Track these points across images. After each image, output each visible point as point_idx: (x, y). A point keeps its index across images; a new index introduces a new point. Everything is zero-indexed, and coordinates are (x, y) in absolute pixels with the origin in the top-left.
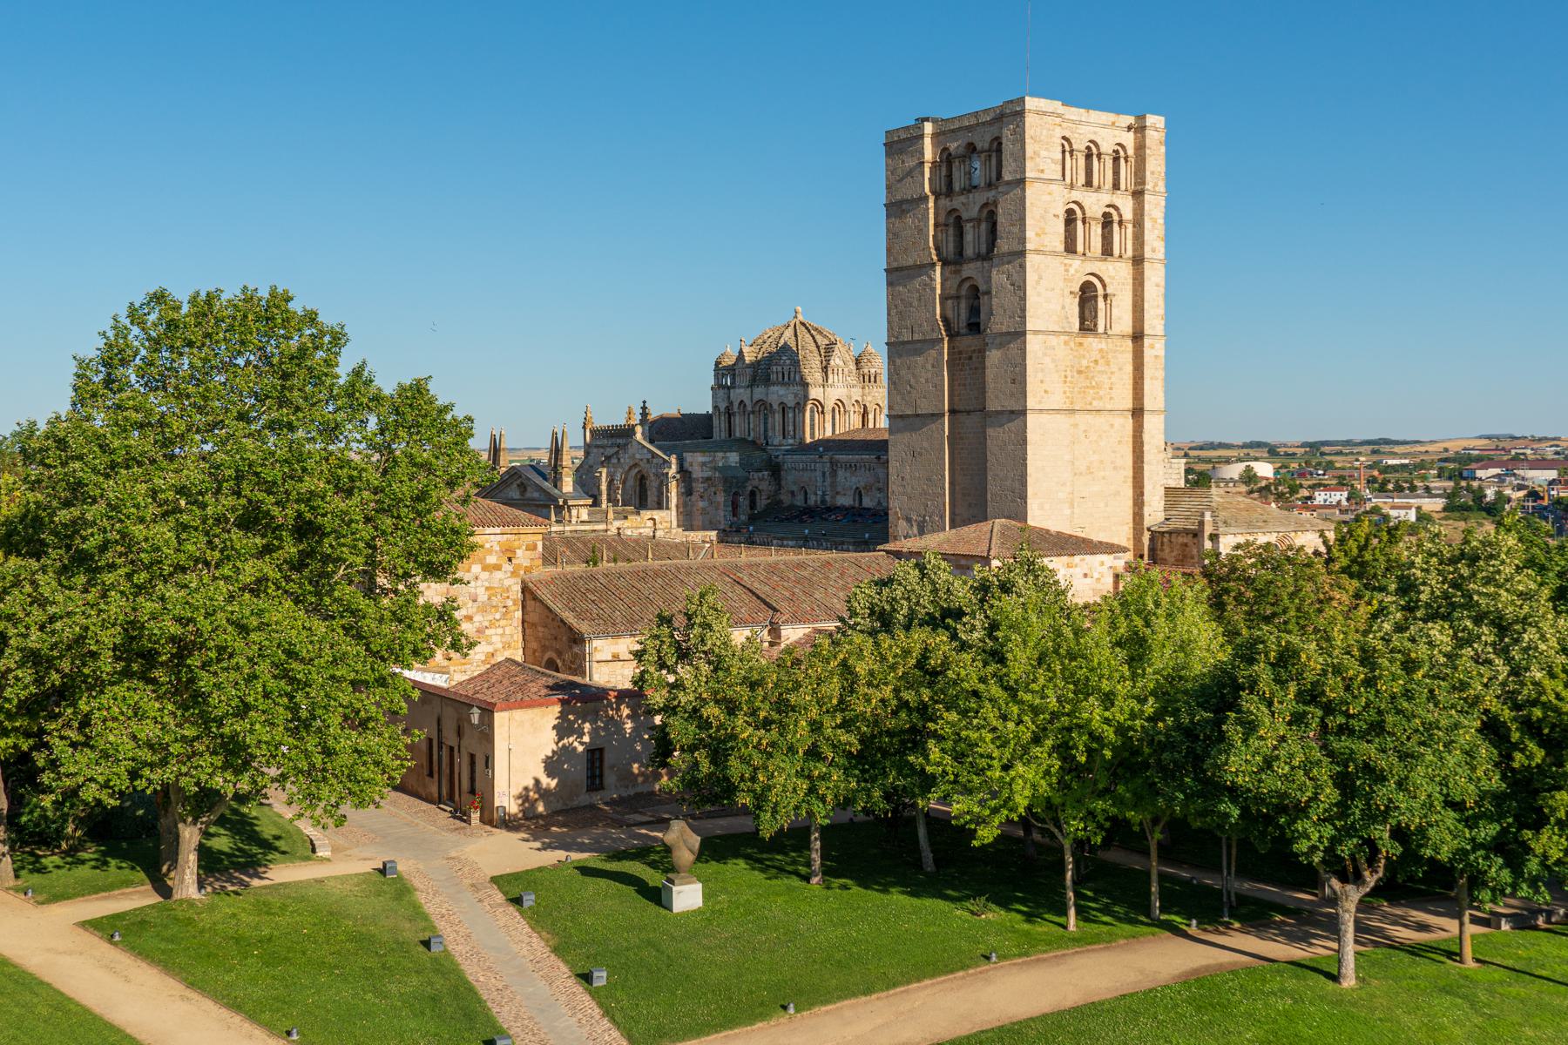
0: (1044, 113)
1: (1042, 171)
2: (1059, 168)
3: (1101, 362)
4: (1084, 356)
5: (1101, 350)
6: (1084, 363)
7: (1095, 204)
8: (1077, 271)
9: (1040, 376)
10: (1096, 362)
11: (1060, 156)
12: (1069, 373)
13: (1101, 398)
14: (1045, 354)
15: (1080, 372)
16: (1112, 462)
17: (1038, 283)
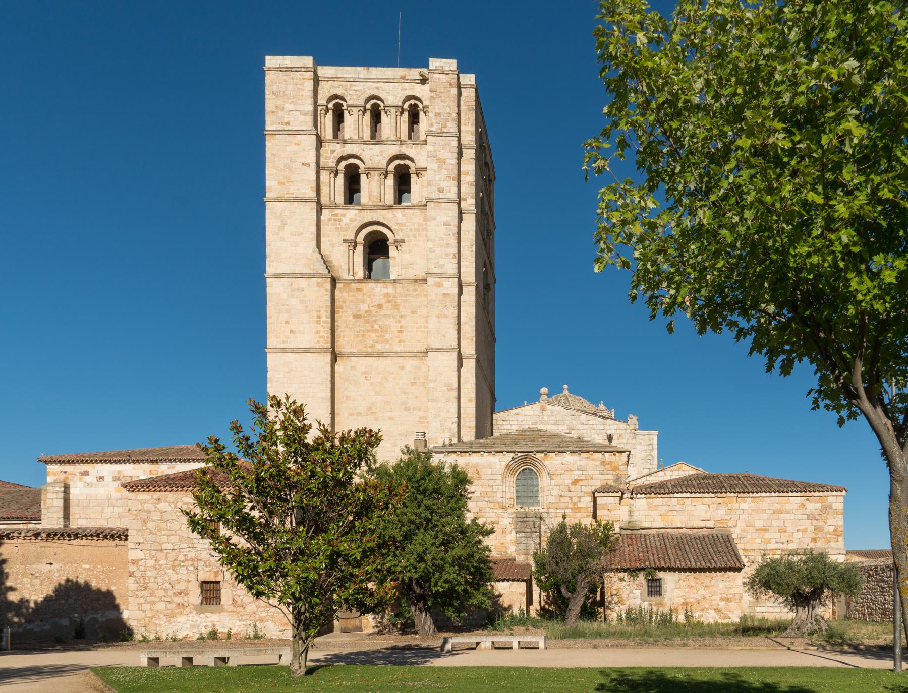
6: (364, 307)
8: (352, 220)
9: (284, 317)
13: (387, 341)
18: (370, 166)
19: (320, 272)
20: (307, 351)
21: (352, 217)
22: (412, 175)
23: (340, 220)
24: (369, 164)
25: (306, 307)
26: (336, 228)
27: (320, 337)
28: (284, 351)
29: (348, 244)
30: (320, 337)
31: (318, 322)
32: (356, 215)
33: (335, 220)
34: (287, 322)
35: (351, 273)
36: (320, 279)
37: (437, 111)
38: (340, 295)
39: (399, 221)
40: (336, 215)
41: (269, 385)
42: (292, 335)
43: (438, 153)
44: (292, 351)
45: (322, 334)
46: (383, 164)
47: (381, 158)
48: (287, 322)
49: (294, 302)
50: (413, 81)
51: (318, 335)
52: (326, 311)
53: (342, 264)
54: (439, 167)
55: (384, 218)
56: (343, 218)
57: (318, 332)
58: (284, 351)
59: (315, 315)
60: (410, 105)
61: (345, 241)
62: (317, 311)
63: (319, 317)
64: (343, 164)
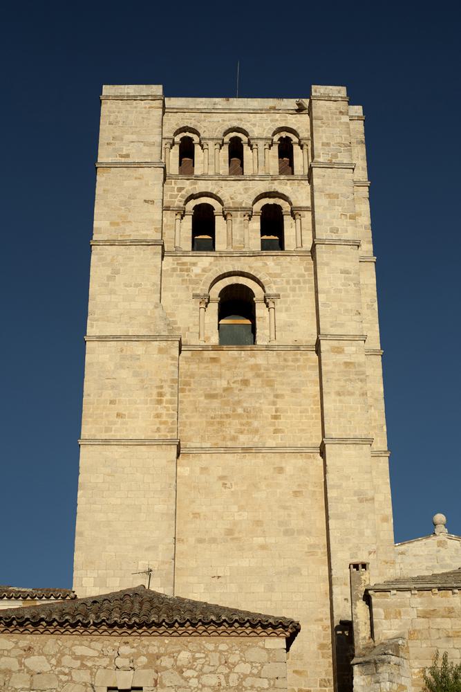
0: (134, 98)
1: (127, 156)
2: (156, 150)
4: (220, 376)
5: (255, 367)
7: (238, 193)
8: (204, 270)
9: (109, 394)
10: (245, 382)
11: (158, 139)
12: (166, 390)
14: (122, 367)
15: (211, 396)
16: (281, 523)
17: (110, 278)
18: (231, 205)
19: (163, 333)
20: (141, 443)
21: (205, 265)
23: (188, 270)
24: (228, 203)
25: (142, 381)
26: (183, 280)
27: (161, 423)
28: (106, 442)
30: (161, 423)
31: (159, 402)
32: (211, 263)
33: (182, 270)
34: (112, 402)
35: (202, 338)
36: (164, 344)
37: (325, 140)
38: (186, 367)
39: (270, 272)
40: (184, 264)
41: (80, 493)
42: (120, 420)
43: (328, 187)
44: (119, 442)
45: (164, 419)
47: (245, 196)
48: (112, 402)
49: (124, 374)
50: (287, 112)
51: (157, 420)
52: (172, 387)
53: (191, 325)
54: (329, 203)
55: (250, 267)
56: (193, 268)
57: (158, 416)
58: (106, 442)
59: (155, 392)
60: (281, 139)
61: (195, 296)
62: (157, 387)
63: (160, 394)
64: (193, 203)
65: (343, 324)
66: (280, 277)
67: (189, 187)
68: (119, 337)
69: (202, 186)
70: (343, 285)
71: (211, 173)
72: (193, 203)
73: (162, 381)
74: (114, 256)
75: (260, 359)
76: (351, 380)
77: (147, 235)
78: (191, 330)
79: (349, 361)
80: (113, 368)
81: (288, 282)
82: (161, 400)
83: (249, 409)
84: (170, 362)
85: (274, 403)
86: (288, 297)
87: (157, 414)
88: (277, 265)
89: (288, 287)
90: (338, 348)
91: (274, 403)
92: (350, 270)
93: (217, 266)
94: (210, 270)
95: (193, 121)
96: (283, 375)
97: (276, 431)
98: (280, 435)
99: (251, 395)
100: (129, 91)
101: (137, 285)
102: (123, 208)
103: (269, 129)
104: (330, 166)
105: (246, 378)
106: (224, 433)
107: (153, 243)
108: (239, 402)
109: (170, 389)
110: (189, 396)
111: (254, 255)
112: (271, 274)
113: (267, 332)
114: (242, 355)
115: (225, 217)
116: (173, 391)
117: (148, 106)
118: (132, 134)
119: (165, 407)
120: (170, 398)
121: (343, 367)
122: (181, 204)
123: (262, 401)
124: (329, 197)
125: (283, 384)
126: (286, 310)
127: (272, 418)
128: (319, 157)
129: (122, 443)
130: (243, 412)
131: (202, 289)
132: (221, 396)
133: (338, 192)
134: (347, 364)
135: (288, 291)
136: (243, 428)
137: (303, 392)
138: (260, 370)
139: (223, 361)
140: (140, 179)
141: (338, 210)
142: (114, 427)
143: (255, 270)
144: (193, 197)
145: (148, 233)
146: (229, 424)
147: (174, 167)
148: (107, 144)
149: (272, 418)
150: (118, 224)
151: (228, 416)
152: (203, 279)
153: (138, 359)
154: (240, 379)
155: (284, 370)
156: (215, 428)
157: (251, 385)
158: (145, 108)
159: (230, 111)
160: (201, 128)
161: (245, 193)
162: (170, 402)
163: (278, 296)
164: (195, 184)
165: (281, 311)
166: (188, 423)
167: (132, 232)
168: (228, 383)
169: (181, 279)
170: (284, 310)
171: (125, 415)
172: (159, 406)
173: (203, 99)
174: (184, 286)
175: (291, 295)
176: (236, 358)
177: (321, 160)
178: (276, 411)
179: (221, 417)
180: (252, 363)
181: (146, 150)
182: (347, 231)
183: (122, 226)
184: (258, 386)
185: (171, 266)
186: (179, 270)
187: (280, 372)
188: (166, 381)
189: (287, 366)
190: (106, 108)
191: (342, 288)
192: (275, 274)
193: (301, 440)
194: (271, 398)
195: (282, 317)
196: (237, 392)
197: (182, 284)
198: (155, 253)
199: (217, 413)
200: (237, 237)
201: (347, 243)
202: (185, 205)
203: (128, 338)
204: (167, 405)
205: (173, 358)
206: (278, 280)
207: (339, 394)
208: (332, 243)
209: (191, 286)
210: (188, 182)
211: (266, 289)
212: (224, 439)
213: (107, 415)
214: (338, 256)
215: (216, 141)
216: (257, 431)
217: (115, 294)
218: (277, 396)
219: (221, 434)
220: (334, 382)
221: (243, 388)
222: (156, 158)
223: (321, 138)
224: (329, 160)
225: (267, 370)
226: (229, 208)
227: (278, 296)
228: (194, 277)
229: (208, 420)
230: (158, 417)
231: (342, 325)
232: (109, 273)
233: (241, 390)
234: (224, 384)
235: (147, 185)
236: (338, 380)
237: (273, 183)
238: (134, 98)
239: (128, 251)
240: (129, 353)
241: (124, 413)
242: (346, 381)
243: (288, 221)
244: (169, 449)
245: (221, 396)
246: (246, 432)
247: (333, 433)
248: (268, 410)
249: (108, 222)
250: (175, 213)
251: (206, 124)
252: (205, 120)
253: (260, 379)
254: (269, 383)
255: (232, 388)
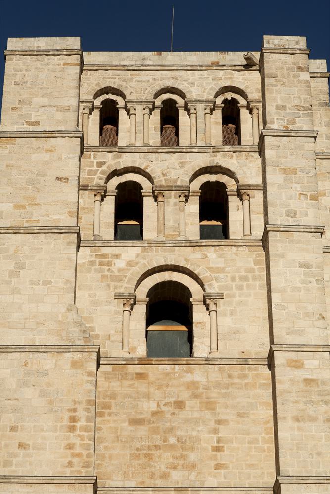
0: (46, 53)
1: (37, 123)
2: (72, 116)
3: (187, 403)
4: (148, 396)
5: (193, 385)
8: (129, 264)
10: (180, 405)
11: (74, 102)
12: (81, 413)
14: (26, 384)
15: (136, 422)
18: (163, 183)
19: (78, 343)
20: (48, 480)
22: (230, 198)
23: (109, 264)
24: (160, 180)
25: (51, 402)
26: (103, 276)
27: (74, 455)
29: (123, 301)
30: (74, 455)
31: (72, 429)
32: (137, 255)
33: (101, 264)
34: (13, 429)
35: (126, 349)
36: (78, 356)
37: (279, 103)
38: (107, 384)
39: (212, 265)
40: (104, 256)
42: (22, 452)
43: (283, 160)
45: (78, 450)
46: (184, 180)
47: (181, 172)
48: (13, 429)
49: (29, 393)
50: (234, 67)
51: (69, 452)
52: (87, 410)
53: (112, 332)
54: (285, 180)
55: (186, 260)
56: (116, 261)
57: (70, 447)
59: (67, 416)
60: (225, 101)
61: (118, 296)
62: (70, 410)
63: (73, 420)
64: (116, 181)
65: (302, 331)
66: (223, 272)
67: (112, 161)
68: (24, 347)
69: (127, 160)
70: (303, 282)
71: (139, 143)
72: (116, 181)
73: (75, 402)
74: (18, 247)
75: (198, 375)
76: (312, 402)
77: (59, 221)
78: (112, 339)
79: (310, 377)
80: (14, 387)
81: (233, 279)
82: (74, 426)
83: (184, 438)
84: (86, 378)
85: (216, 431)
86: (234, 296)
87: (69, 444)
88: (220, 256)
89: (234, 284)
90: (296, 361)
91: (216, 431)
92: (311, 263)
93: (145, 259)
94: (137, 263)
95: (117, 80)
96: (225, 395)
97: (218, 467)
98: (222, 471)
99: (187, 421)
100: (40, 44)
101: (47, 283)
102: (30, 187)
103: (211, 89)
104: (286, 133)
105: (179, 399)
106: (153, 469)
107: (67, 231)
108: (171, 430)
109: (85, 413)
110: (109, 421)
111: (191, 244)
112: (212, 268)
113: (207, 341)
114: (176, 371)
115: (156, 198)
116: (89, 415)
117: (62, 62)
118: (42, 97)
119: (79, 436)
120: (85, 424)
121: (302, 386)
122: (102, 182)
123: (200, 429)
124: (285, 173)
125: (227, 407)
126: (231, 314)
127: (213, 450)
128: (272, 123)
129: (25, 481)
130: (176, 442)
131: (126, 287)
132: (149, 422)
133: (296, 167)
134: (308, 382)
135: (234, 290)
136: (176, 462)
137: (252, 417)
138: (198, 388)
139: (152, 378)
140: (51, 151)
141: (296, 188)
142: (15, 461)
143: (192, 264)
144: (116, 173)
145: (61, 217)
146: (160, 457)
147: (93, 136)
148: (12, 109)
149: (213, 450)
150: (23, 207)
151: (157, 447)
152: (128, 274)
153: (47, 375)
154: (172, 400)
155: (227, 388)
156: (140, 462)
157: (187, 408)
158: (59, 65)
159: (163, 67)
160: (126, 88)
161: (181, 167)
162: (86, 429)
163: (221, 296)
164: (120, 157)
165: (225, 315)
166: (107, 456)
167: (41, 217)
168: (158, 405)
169: (100, 275)
170: (228, 313)
171: (29, 445)
172: (72, 434)
173: (130, 54)
174: (104, 284)
175: (237, 295)
176: (168, 374)
177: (275, 126)
178: (218, 441)
179: (149, 448)
180: (188, 380)
181: (59, 116)
182: (307, 215)
183: (28, 209)
184: (196, 409)
185: (89, 259)
186: (98, 264)
187: (223, 391)
188: (80, 403)
189: (232, 384)
190: (11, 65)
191: (301, 285)
192: (217, 268)
193: (249, 478)
194: (212, 424)
195: (226, 322)
196: (168, 416)
197: (102, 282)
198: (69, 243)
199: (144, 443)
200: (170, 223)
201: (307, 229)
202: (106, 183)
203: (34, 349)
204: (81, 434)
205: (90, 374)
206: (221, 275)
207: (297, 420)
208: (288, 230)
209: (112, 284)
210: (110, 155)
211: (206, 287)
212: (152, 476)
213: (6, 445)
214: (297, 245)
215: (145, 105)
216: (193, 466)
217: (19, 293)
218: (219, 422)
219: (148, 469)
220: (291, 404)
221: (176, 411)
222: (71, 126)
223: (274, 99)
224: (285, 127)
225: (207, 388)
226: (161, 186)
227: (221, 296)
228: (116, 273)
229: (132, 452)
230: (70, 448)
231: (300, 332)
232: (12, 266)
233: (174, 414)
234: (153, 406)
235: (60, 159)
236: (296, 402)
237: (216, 156)
238: (46, 53)
239: (36, 241)
240: (35, 367)
241: (28, 442)
242: (306, 403)
243: (233, 202)
244: (83, 488)
245: (149, 422)
246: (180, 467)
247: (290, 469)
248: (208, 440)
249: (12, 204)
250: (94, 193)
251: (132, 84)
252: (131, 79)
253: (198, 401)
254: (210, 406)
255: (162, 412)
